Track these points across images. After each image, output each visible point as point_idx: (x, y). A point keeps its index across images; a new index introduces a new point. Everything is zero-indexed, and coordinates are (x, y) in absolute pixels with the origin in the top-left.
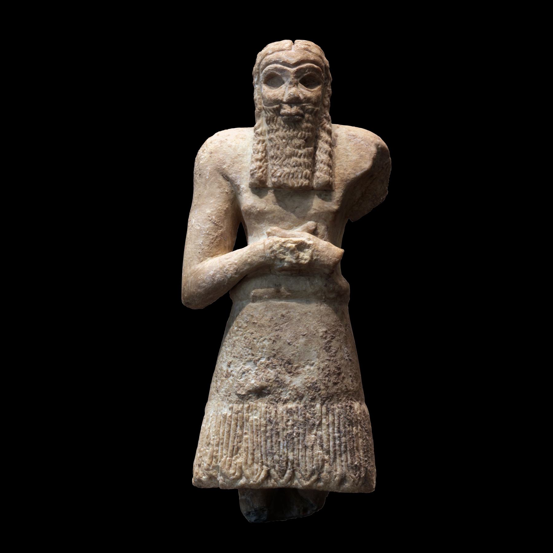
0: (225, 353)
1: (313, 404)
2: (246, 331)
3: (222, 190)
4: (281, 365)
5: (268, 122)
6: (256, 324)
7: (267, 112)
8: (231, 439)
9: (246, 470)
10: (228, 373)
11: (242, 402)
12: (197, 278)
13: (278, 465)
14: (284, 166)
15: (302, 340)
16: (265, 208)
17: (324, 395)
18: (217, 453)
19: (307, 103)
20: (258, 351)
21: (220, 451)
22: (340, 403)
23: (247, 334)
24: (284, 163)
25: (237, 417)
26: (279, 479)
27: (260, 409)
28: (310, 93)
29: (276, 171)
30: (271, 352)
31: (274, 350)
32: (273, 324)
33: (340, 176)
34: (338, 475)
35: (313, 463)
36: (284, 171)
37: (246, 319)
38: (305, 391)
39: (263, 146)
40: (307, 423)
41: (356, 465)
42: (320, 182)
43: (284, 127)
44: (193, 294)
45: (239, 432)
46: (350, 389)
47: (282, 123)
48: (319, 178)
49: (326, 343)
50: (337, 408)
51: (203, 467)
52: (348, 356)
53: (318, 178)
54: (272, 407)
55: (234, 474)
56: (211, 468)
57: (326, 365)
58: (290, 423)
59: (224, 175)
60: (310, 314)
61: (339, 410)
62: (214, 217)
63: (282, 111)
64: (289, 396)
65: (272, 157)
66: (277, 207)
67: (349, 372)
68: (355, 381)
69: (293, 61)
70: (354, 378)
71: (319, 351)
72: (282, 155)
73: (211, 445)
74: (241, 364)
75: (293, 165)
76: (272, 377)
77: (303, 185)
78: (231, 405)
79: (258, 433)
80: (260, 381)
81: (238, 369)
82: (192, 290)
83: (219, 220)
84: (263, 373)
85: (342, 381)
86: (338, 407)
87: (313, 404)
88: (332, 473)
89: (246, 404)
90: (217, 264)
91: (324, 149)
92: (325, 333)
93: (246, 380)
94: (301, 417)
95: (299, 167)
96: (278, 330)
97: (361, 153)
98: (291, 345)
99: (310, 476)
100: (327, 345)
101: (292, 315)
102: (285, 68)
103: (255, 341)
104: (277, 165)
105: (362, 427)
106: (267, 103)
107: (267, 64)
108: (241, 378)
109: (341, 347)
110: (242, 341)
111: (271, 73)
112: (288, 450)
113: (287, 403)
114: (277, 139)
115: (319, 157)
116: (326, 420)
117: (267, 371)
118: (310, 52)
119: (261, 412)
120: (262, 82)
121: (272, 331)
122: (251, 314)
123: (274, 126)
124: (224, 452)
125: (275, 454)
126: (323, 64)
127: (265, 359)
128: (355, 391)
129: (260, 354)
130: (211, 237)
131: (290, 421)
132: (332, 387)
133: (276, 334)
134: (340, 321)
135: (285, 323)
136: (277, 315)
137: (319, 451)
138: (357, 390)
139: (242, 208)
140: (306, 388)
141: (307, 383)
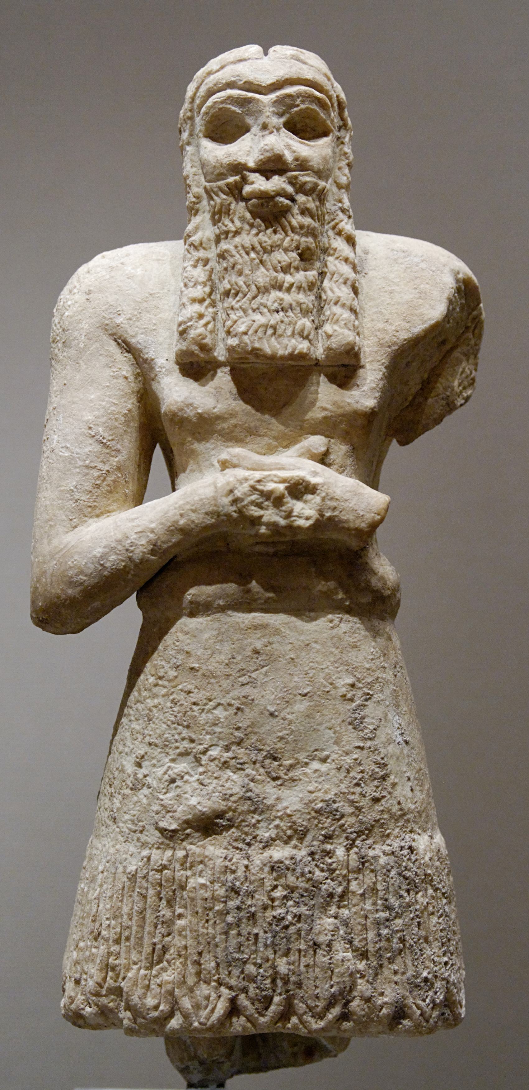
0: (128, 734)
1: (328, 847)
2: (175, 687)
3: (114, 372)
4: (254, 763)
5: (216, 217)
6: (198, 671)
7: (213, 195)
8: (147, 929)
9: (184, 999)
10: (136, 779)
11: (172, 845)
12: (66, 563)
13: (254, 985)
14: (254, 311)
15: (301, 706)
16: (214, 408)
17: (352, 827)
18: (116, 959)
19: (302, 171)
20: (204, 732)
21: (123, 954)
22: (388, 842)
23: (177, 694)
24: (255, 305)
25: (161, 879)
26: (256, 1015)
27: (212, 862)
28: (307, 148)
29: (235, 322)
30: (232, 734)
31: (238, 729)
32: (236, 671)
33: (376, 335)
34: (386, 1003)
35: (331, 979)
36: (254, 321)
37: (175, 661)
38: (309, 819)
39: (205, 271)
40: (318, 892)
41: (426, 980)
42: (334, 346)
43: (252, 226)
44: (56, 600)
45: (166, 913)
46: (409, 809)
47: (248, 215)
48: (331, 336)
49: (354, 711)
50: (381, 854)
51: (85, 985)
52: (402, 734)
53: (329, 336)
54: (237, 856)
55: (156, 1007)
56: (104, 992)
57: (356, 759)
58: (278, 893)
59: (120, 338)
60: (318, 646)
61: (386, 858)
62: (101, 429)
63: (247, 189)
64: (275, 831)
65: (227, 294)
66: (240, 406)
67: (405, 769)
68: (418, 788)
69: (267, 79)
70: (416, 782)
71: (338, 729)
72: (248, 286)
73: (103, 938)
74: (167, 760)
75: (273, 308)
76: (236, 789)
77: (296, 352)
78: (145, 853)
79: (208, 915)
80: (209, 799)
81: (160, 771)
82: (53, 591)
83: (112, 435)
84: (215, 781)
85: (390, 793)
86: (384, 853)
87: (328, 847)
88: (374, 999)
89: (180, 849)
90: (110, 532)
91: (342, 275)
92: (350, 688)
93: (178, 796)
94: (304, 879)
95: (287, 311)
96: (247, 684)
97: (422, 286)
98: (277, 716)
99: (328, 1008)
100: (356, 715)
101: (277, 650)
102: (250, 95)
103: (195, 708)
104: (237, 310)
105: (436, 890)
106: (212, 173)
107: (210, 93)
108: (165, 793)
109: (386, 716)
110: (167, 708)
111: (220, 109)
112: (275, 952)
113: (271, 846)
114: (238, 252)
115: (329, 293)
116: (359, 884)
117: (226, 776)
118: (305, 63)
119: (213, 868)
120: (201, 135)
121: (233, 686)
122: (186, 648)
123: (230, 225)
124: (134, 957)
125: (245, 963)
126: (333, 92)
127: (219, 749)
128: (418, 812)
129: (208, 737)
130: (96, 474)
131: (280, 888)
132: (370, 808)
133: (243, 694)
134: (382, 659)
135: (263, 667)
136: (244, 650)
137: (345, 954)
138: (423, 808)
139: (163, 409)
140: (313, 814)
141: (314, 801)
